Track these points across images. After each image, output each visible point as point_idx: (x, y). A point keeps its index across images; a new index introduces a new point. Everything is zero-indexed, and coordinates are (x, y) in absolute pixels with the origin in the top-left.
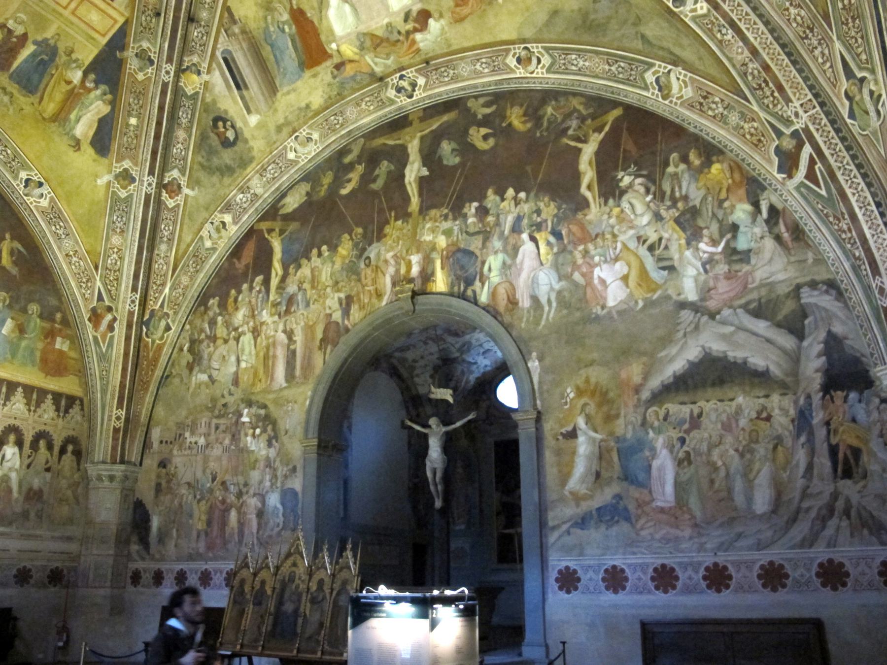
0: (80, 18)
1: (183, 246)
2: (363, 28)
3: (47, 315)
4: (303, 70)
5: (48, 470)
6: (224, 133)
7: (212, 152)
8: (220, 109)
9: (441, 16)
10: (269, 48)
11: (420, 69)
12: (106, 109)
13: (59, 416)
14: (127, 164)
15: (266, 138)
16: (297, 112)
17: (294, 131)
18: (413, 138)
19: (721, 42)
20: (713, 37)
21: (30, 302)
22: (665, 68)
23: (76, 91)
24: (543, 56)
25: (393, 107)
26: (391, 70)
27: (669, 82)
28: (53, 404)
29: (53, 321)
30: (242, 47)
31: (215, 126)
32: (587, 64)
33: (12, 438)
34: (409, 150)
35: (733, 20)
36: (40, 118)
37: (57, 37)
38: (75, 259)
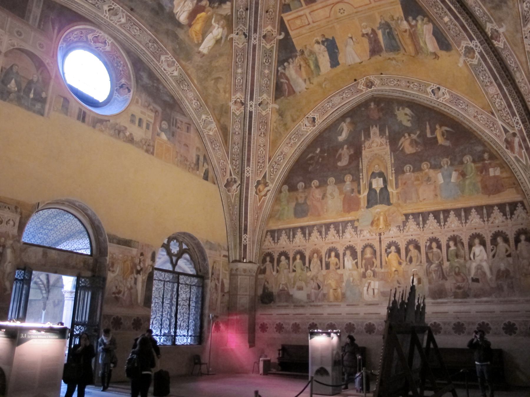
1: (525, 66)
3: (478, 159)
5: (509, 256)
12: (430, 26)
13: (507, 218)
14: (464, 44)
21: (463, 157)
23: (411, 31)
28: (500, 212)
29: (484, 160)
33: (477, 241)
37: (382, 18)
38: (479, 116)
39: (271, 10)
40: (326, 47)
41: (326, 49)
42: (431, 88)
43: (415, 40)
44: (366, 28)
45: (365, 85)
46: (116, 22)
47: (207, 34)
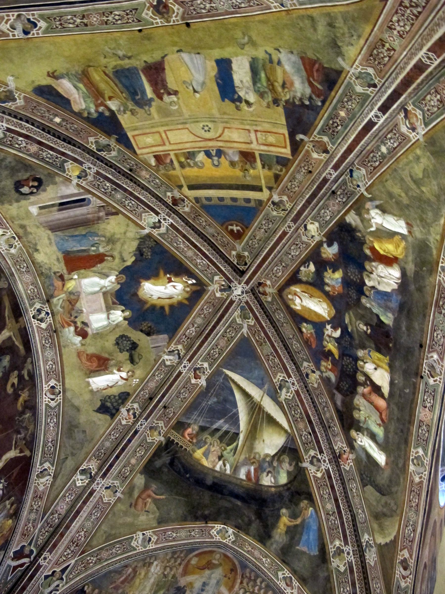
0: (154, 133)
2: (83, 296)
4: (63, 253)
6: (28, 185)
7: (13, 170)
8: (48, 186)
9: (83, 345)
10: (84, 233)
11: (51, 326)
12: (76, 108)
15: (18, 217)
16: (33, 242)
17: (19, 238)
18: (10, 330)
19: (65, 496)
20: (66, 492)
22: (52, 472)
23: (102, 99)
24: (55, 402)
25: (28, 305)
26: (53, 308)
27: (45, 476)
30: (88, 214)
31: (35, 179)
32: (52, 428)
34: (3, 332)
35: (80, 512)
36: (91, 64)
37: (148, 113)
39: (304, 171)
40: (235, 92)
41: (237, 89)
42: (40, 28)
43: (93, 89)
44: (171, 102)
45: (171, 10)
46: (440, 367)
47: (388, 231)
